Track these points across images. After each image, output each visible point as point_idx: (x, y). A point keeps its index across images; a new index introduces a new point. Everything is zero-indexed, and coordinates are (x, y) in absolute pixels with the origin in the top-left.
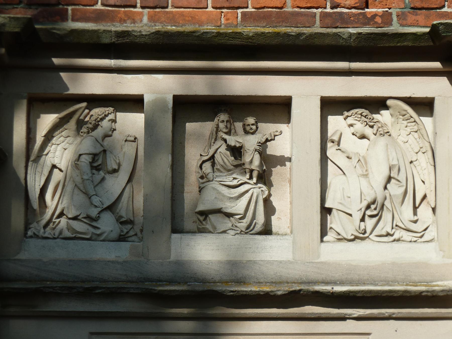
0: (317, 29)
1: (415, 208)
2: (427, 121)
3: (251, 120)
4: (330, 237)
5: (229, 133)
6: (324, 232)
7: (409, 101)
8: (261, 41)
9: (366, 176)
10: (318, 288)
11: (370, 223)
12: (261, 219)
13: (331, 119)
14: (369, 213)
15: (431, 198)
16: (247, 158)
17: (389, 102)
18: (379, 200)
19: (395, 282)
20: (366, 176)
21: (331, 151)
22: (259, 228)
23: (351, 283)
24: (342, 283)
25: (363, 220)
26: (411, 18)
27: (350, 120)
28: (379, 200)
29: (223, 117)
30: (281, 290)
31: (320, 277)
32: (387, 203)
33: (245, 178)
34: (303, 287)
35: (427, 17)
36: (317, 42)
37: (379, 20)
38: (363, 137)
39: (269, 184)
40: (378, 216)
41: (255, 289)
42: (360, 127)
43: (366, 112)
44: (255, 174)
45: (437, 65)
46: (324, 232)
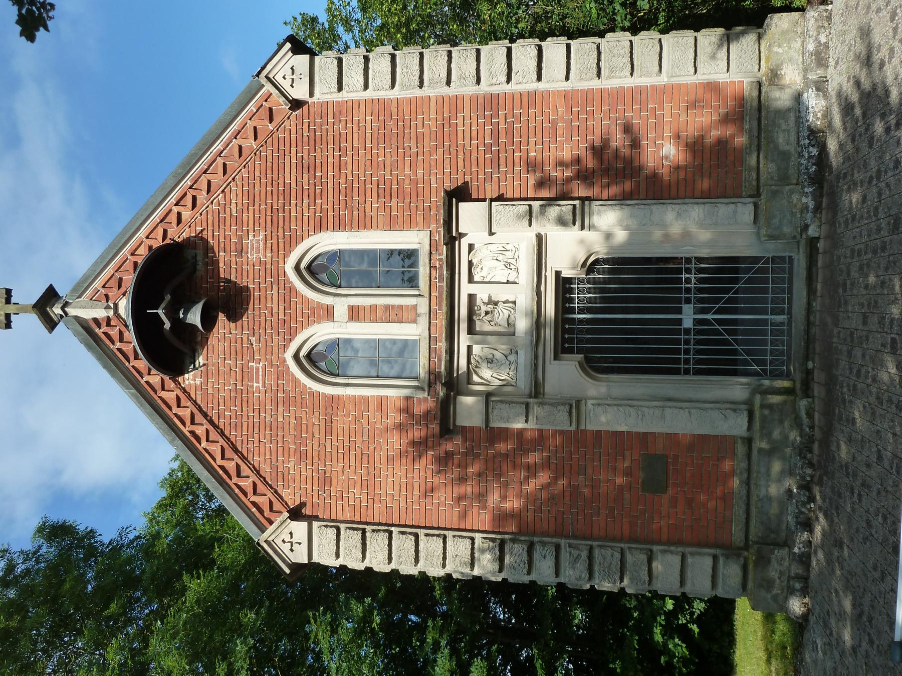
0: (444, 284)
1: (507, 251)
2: (476, 246)
3: (476, 308)
4: (517, 281)
5: (480, 316)
6: (516, 283)
7: (469, 252)
8: (449, 304)
9: (495, 268)
10: (535, 286)
11: (512, 267)
12: (510, 305)
13: (475, 280)
14: (508, 267)
15: (503, 245)
16: (489, 310)
17: (470, 260)
18: (504, 263)
19: (533, 258)
20: (495, 268)
21: (487, 280)
22: (514, 306)
23: (533, 274)
24: (533, 277)
25: (511, 269)
26: (440, 251)
27: (476, 273)
28: (504, 263)
29: (474, 318)
30: (536, 298)
31: (531, 284)
32: (505, 260)
33: (496, 310)
34: (535, 291)
35: (440, 246)
36: (449, 285)
37: (441, 263)
38: (482, 269)
39: (498, 302)
40: (510, 264)
41: (535, 308)
42: (478, 270)
43: (473, 267)
44: (495, 307)
45: (457, 243)
46: (516, 283)
